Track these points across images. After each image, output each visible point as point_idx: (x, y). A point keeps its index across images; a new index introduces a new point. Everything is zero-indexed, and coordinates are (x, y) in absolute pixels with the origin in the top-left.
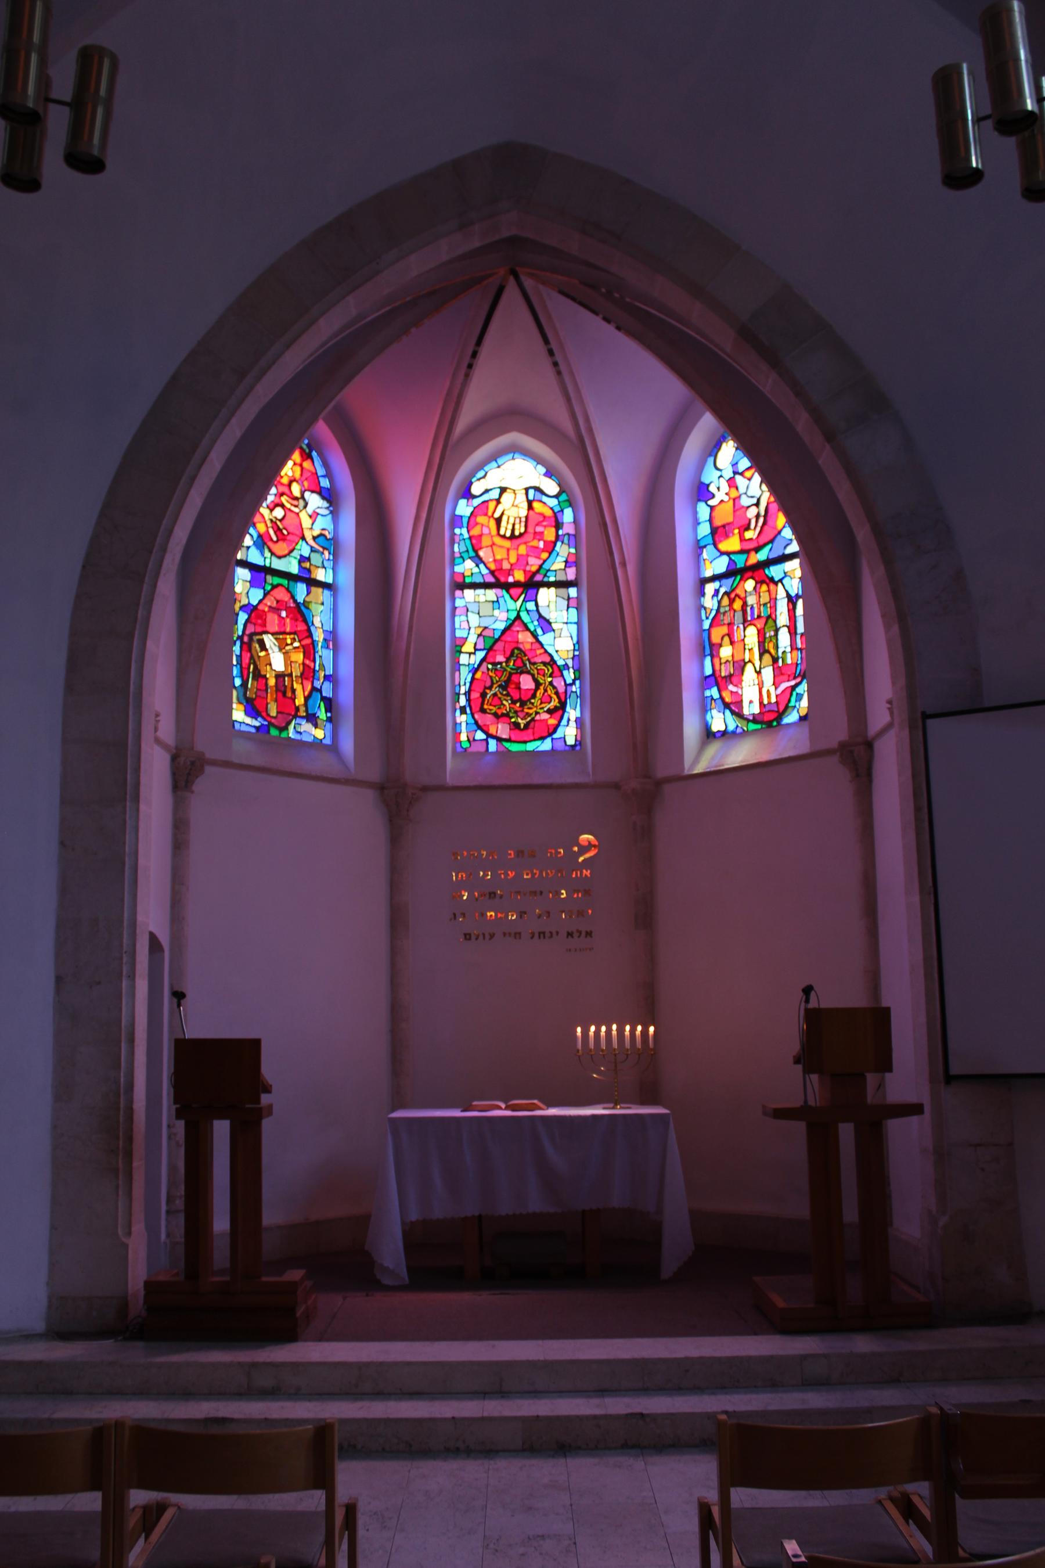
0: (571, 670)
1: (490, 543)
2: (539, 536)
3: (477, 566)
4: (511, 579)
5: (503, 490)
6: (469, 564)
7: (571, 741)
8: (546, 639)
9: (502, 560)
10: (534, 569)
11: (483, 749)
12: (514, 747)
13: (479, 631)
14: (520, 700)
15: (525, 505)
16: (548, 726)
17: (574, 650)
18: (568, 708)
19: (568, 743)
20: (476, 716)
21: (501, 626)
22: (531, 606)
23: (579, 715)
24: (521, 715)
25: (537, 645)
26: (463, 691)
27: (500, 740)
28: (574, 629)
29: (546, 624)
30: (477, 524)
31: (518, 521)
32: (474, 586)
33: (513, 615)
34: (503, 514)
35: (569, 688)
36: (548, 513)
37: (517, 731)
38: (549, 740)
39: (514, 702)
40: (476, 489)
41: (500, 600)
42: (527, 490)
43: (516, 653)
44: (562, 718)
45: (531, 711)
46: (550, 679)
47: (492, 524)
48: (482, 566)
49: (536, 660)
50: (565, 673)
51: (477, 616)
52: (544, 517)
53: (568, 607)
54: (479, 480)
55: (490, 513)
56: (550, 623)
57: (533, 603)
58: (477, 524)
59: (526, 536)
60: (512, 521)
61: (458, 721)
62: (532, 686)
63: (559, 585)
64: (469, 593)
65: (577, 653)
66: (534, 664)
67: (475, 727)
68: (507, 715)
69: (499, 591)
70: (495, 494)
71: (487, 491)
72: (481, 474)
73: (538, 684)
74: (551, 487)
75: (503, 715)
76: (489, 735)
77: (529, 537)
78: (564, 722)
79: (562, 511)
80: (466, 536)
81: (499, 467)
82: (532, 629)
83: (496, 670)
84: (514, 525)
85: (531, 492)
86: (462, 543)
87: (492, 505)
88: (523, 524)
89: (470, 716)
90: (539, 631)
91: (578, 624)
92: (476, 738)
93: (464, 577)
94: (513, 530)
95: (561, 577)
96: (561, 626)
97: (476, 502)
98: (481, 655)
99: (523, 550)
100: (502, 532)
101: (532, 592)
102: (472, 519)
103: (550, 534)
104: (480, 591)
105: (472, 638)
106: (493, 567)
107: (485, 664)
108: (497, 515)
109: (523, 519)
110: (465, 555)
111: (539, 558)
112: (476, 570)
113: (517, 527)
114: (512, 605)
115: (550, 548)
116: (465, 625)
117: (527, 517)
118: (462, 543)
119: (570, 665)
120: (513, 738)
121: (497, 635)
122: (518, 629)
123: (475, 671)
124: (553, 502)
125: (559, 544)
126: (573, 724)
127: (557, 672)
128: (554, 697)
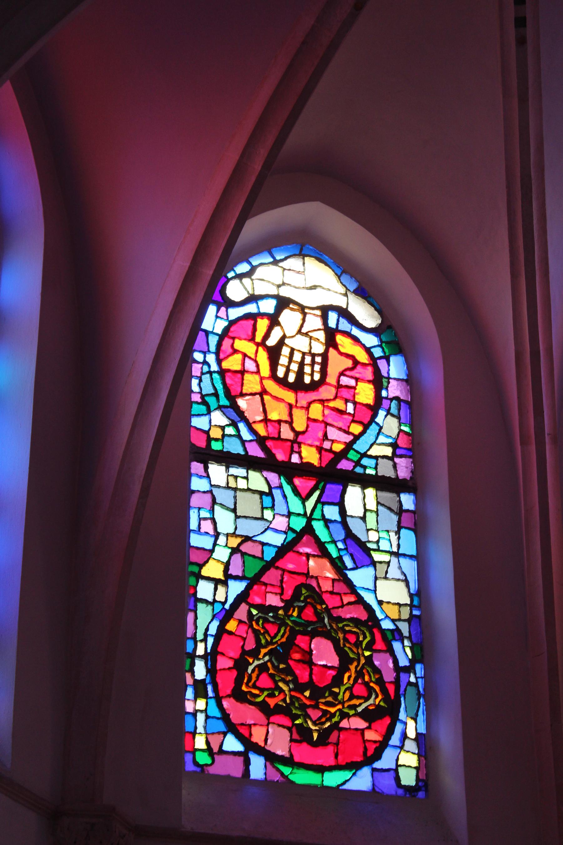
0: (406, 643)
1: (258, 388)
2: (345, 392)
3: (234, 424)
4: (295, 459)
5: (283, 303)
6: (218, 418)
7: (408, 778)
8: (361, 577)
9: (279, 422)
10: (338, 447)
11: (237, 772)
12: (302, 777)
13: (234, 542)
14: (310, 685)
15: (321, 336)
16: (365, 741)
17: (411, 606)
18: (402, 715)
19: (403, 783)
20: (225, 704)
21: (278, 540)
22: (332, 512)
23: (422, 729)
24: (315, 714)
25: (341, 587)
26: (200, 651)
27: (271, 758)
28: (410, 567)
29: (362, 552)
30: (235, 351)
31: (308, 360)
32: (227, 459)
33: (299, 524)
34: (281, 342)
35: (403, 676)
36: (362, 357)
37: (305, 746)
38: (366, 772)
39: (299, 688)
40: (235, 290)
41: (277, 493)
42: (325, 310)
43: (306, 593)
44: (390, 731)
45: (333, 710)
46: (367, 653)
47: (263, 357)
48: (242, 426)
49: (341, 613)
50: (397, 646)
51: (231, 516)
52: (356, 363)
53: (400, 527)
54: (240, 277)
55: (258, 339)
56: (367, 551)
57: (336, 509)
58: (235, 351)
59: (323, 389)
60: (297, 357)
61: (189, 707)
62: (333, 660)
63: (380, 483)
64: (217, 472)
65: (416, 612)
66: (340, 619)
67: (221, 726)
68: (284, 710)
69: (273, 477)
70: (268, 306)
71: (253, 299)
72: (243, 268)
73: (345, 662)
74: (366, 315)
75: (278, 710)
76: (251, 746)
77: (327, 392)
78: (395, 740)
79: (387, 358)
80: (214, 367)
81: (276, 262)
82: (334, 554)
83: (266, 621)
84: (302, 364)
85: (333, 317)
86: (206, 378)
87: (262, 325)
88: (317, 368)
89: (212, 702)
90: (349, 563)
91: (420, 558)
92: (225, 748)
93: (209, 440)
94: (300, 373)
95: (386, 470)
96: (386, 557)
97: (235, 313)
98: (236, 588)
99: (316, 411)
100: (281, 373)
101: (333, 489)
102: (227, 343)
103: (365, 393)
104: (241, 472)
105: (222, 554)
106: (261, 430)
107: (244, 607)
108: (272, 342)
109: (318, 359)
110: (212, 401)
111: (347, 432)
112: (230, 431)
113: (307, 369)
114: (295, 504)
115: (368, 415)
116: (207, 526)
117: (325, 356)
118: (206, 378)
119: (406, 633)
120: (297, 759)
121: (270, 554)
122: (308, 550)
123: (226, 616)
124: (370, 340)
125: (382, 413)
126: (410, 745)
127: (380, 645)
128: (377, 689)
